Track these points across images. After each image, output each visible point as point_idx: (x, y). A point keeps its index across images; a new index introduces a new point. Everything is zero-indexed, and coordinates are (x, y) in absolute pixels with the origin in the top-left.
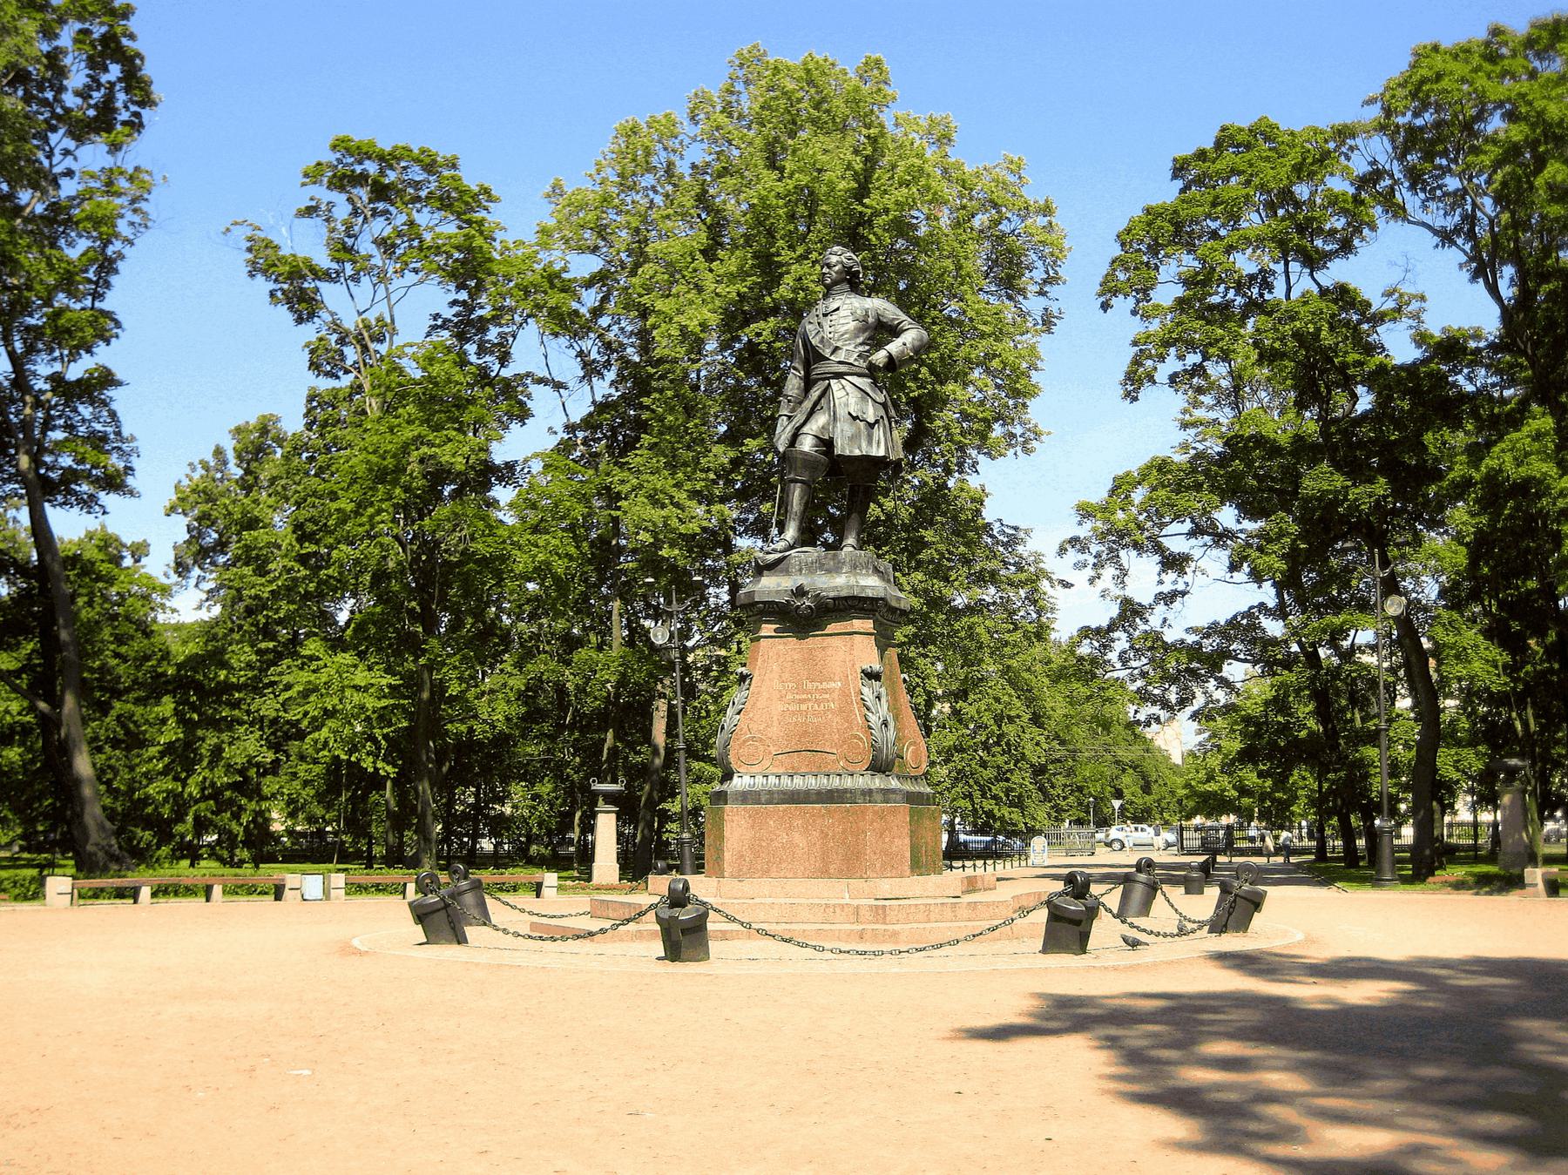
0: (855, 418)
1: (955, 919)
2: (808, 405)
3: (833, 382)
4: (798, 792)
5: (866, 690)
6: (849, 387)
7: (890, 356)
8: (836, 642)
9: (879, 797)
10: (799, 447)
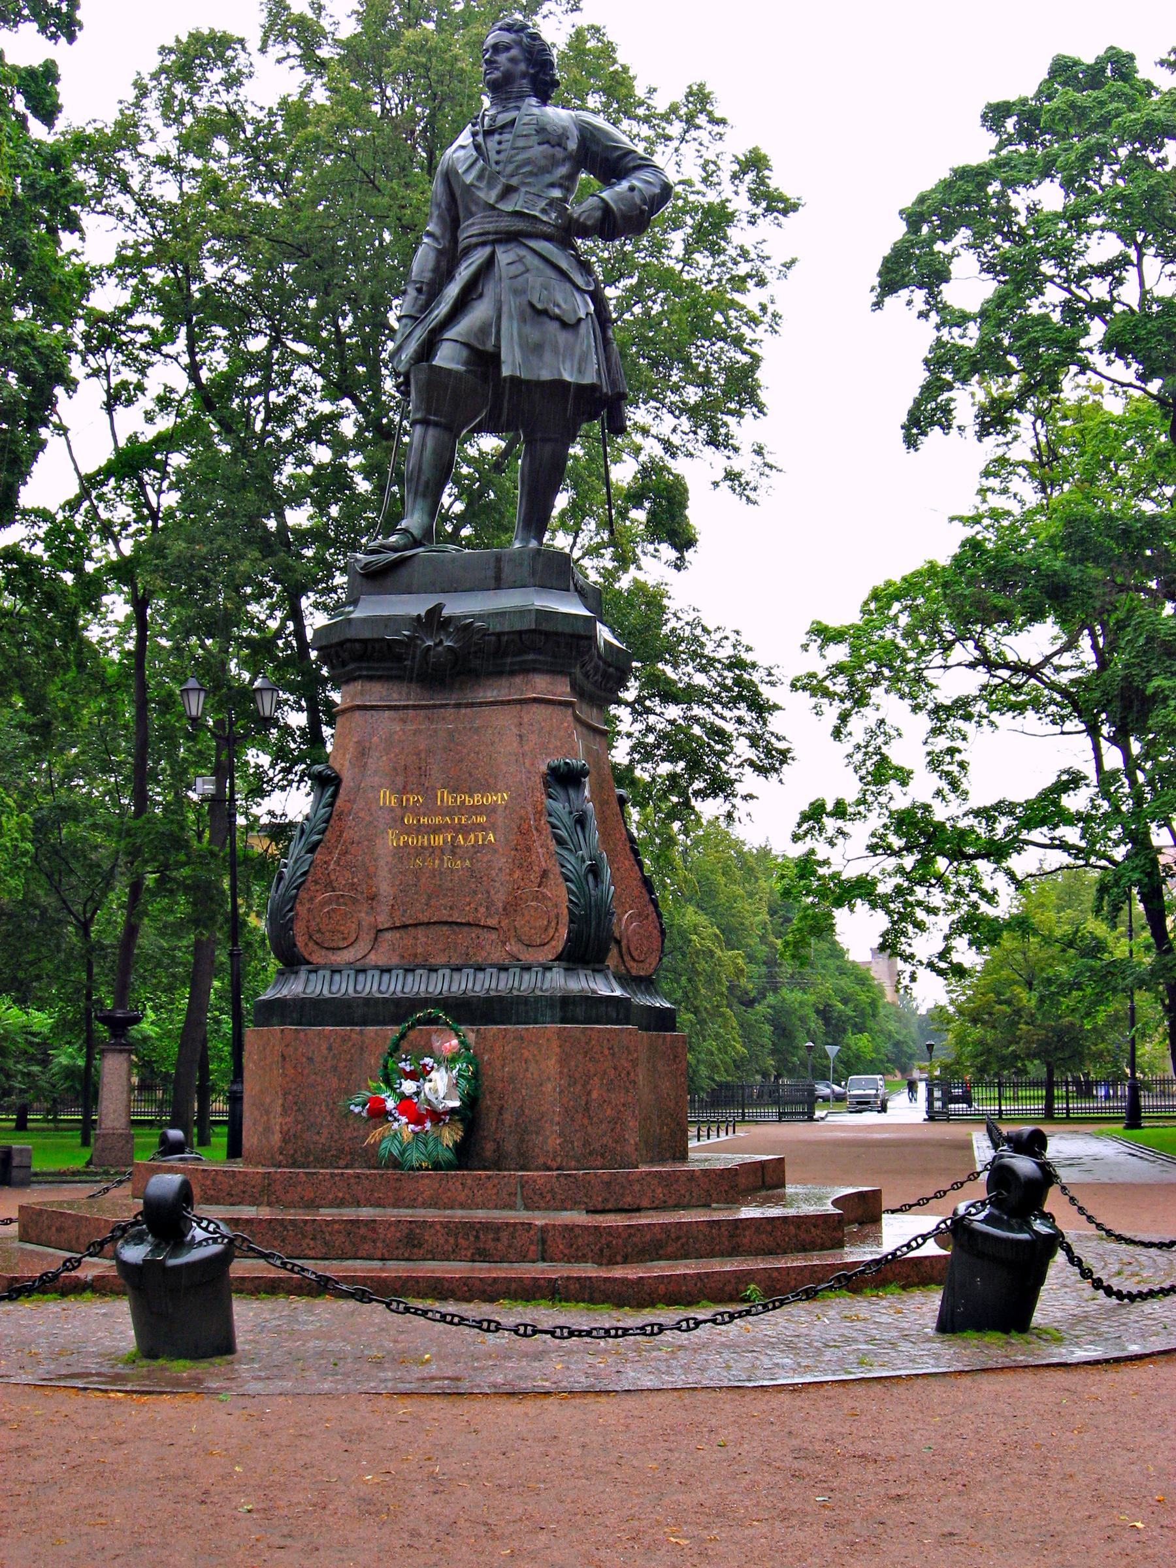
0: (544, 313)
2: (453, 290)
3: (499, 250)
6: (532, 261)
7: (606, 208)
8: (504, 719)
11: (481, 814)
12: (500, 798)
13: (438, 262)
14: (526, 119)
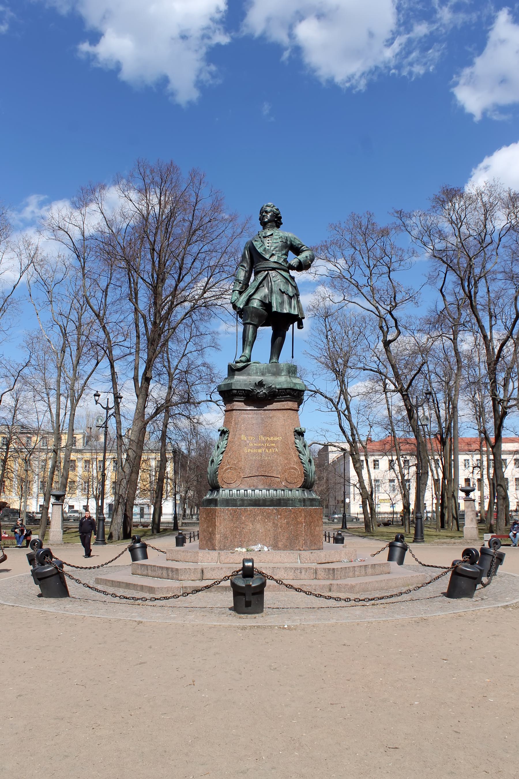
0: (283, 293)
1: (366, 574)
3: (270, 272)
4: (259, 500)
5: (297, 441)
7: (300, 262)
8: (279, 414)
9: (308, 503)
10: (251, 305)
11: (273, 443)
12: (279, 438)
13: (245, 274)
14: (276, 234)
